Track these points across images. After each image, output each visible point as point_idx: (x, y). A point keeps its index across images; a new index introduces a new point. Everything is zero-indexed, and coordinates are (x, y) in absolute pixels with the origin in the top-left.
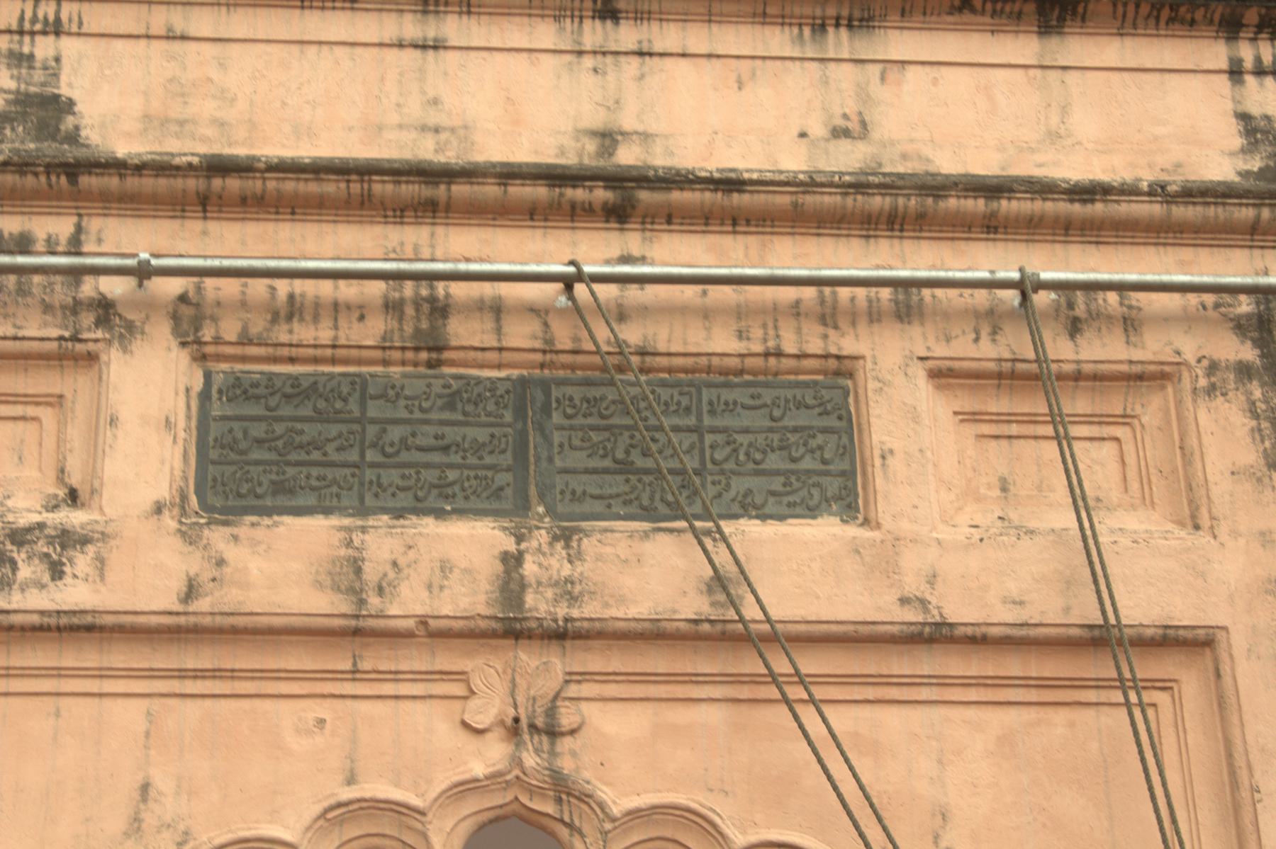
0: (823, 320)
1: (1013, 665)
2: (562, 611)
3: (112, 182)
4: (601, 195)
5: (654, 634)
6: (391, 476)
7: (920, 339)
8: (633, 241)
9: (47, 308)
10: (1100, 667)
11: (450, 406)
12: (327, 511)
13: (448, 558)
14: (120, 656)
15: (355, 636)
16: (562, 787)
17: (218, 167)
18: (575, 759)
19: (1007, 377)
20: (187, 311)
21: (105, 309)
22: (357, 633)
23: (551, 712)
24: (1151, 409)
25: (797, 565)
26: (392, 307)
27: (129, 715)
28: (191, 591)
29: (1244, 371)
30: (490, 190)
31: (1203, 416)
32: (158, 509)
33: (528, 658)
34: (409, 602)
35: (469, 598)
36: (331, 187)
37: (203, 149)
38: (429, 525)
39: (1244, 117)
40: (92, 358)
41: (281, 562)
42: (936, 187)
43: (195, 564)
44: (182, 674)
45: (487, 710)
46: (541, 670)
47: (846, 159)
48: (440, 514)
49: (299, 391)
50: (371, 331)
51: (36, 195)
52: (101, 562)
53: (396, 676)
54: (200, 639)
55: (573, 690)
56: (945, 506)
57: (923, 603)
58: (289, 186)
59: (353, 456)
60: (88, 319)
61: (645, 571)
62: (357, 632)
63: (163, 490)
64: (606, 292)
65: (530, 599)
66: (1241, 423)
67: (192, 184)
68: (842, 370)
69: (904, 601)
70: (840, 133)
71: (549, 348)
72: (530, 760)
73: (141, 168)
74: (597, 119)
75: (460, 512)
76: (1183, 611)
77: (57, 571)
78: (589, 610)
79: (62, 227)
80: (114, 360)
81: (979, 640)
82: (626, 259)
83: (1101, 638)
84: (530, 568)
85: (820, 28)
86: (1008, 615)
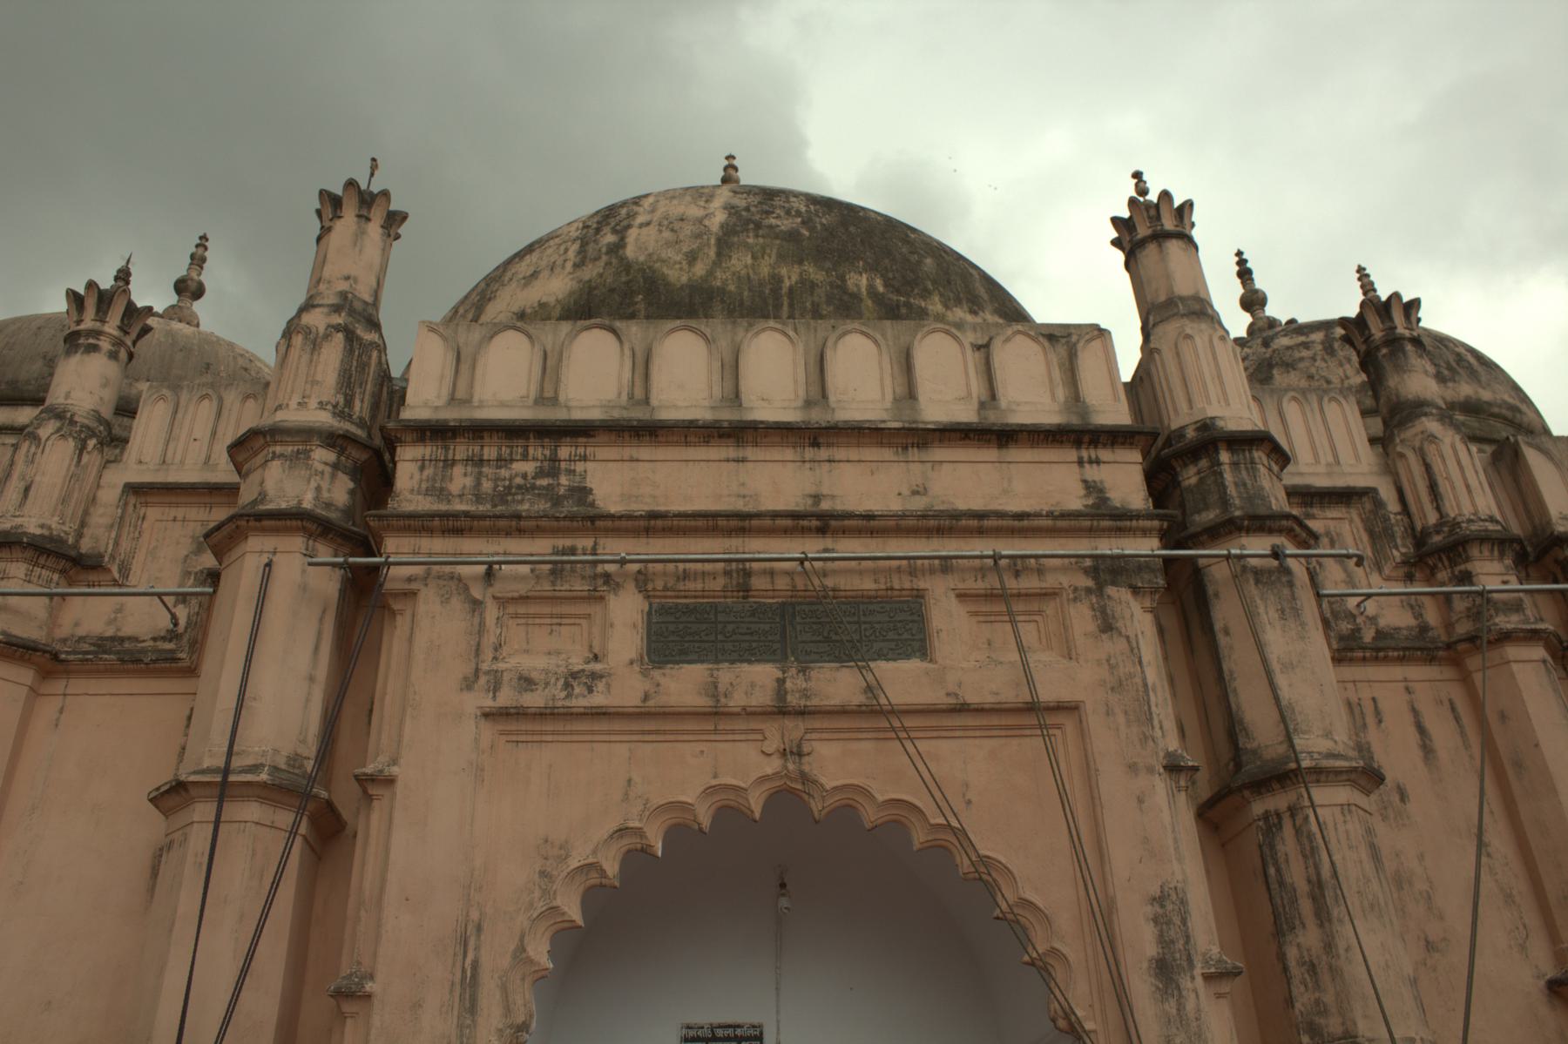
0: (910, 574)
1: (995, 720)
2: (802, 703)
3: (609, 523)
4: (815, 523)
5: (843, 712)
6: (729, 646)
7: (952, 581)
8: (828, 542)
9: (583, 578)
10: (1030, 720)
11: (753, 615)
12: (702, 662)
13: (754, 681)
14: (617, 725)
15: (715, 715)
16: (804, 778)
17: (653, 515)
19: (990, 596)
20: (641, 577)
21: (607, 577)
23: (799, 746)
24: (1050, 608)
25: (902, 680)
26: (727, 573)
27: (622, 750)
28: (646, 698)
29: (1088, 590)
30: (768, 522)
31: (1072, 611)
32: (632, 663)
33: (789, 723)
34: (737, 701)
35: (763, 698)
36: (700, 523)
37: (647, 508)
38: (745, 666)
39: (1085, 481)
40: (602, 598)
41: (684, 684)
42: (956, 515)
43: (648, 686)
44: (643, 732)
45: (772, 745)
46: (795, 728)
47: (918, 504)
48: (750, 662)
49: (689, 610)
50: (720, 583)
51: (578, 530)
52: (608, 686)
53: (733, 732)
55: (808, 736)
56: (966, 652)
57: (956, 695)
58: (683, 523)
59: (712, 638)
60: (600, 581)
61: (837, 684)
62: (716, 713)
63: (633, 655)
64: (817, 564)
65: (789, 698)
66: (1088, 613)
67: (642, 523)
68: (919, 595)
69: (948, 694)
70: (915, 493)
71: (794, 589)
72: (791, 766)
73: (621, 517)
74: (811, 490)
75: (758, 661)
76: (1065, 695)
77: (590, 690)
78: (815, 702)
79: (588, 543)
80: (613, 601)
81: (980, 710)
82: (826, 550)
83: (1032, 708)
84: (788, 684)
85: (905, 448)
86: (991, 699)
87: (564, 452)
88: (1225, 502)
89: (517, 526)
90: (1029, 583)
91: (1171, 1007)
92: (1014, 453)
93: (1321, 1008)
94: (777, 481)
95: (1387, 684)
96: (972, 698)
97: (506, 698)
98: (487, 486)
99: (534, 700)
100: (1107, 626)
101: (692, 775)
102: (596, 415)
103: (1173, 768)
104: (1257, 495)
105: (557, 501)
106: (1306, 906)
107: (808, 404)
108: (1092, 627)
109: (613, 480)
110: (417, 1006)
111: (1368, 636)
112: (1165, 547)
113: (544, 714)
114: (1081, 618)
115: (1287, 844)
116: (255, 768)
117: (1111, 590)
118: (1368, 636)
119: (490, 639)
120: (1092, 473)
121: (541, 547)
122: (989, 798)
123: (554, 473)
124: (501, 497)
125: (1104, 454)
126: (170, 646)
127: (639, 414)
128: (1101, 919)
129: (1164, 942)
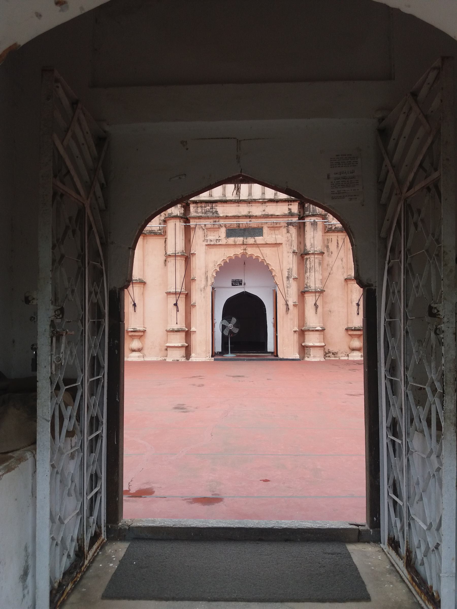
5: (251, 244)
13: (240, 240)
15: (235, 245)
16: (246, 253)
17: (227, 216)
18: (247, 251)
19: (272, 227)
22: (235, 245)
25: (259, 240)
33: (244, 246)
34: (238, 243)
35: (241, 243)
41: (231, 240)
43: (226, 241)
46: (245, 246)
47: (264, 213)
49: (232, 230)
54: (227, 245)
56: (268, 236)
61: (250, 240)
68: (262, 227)
81: (269, 244)
83: (276, 244)
87: (214, 205)
88: (310, 211)
89: (208, 218)
90: (278, 225)
91: (288, 282)
92: (279, 204)
93: (308, 282)
94: (243, 210)
95: (334, 237)
96: (268, 243)
97: (209, 243)
98: (203, 211)
99: (212, 243)
100: (288, 232)
101: (232, 252)
102: (218, 199)
103: (294, 252)
104: (314, 210)
105: (213, 213)
106: (308, 270)
107: (249, 196)
108: (286, 232)
109: (222, 210)
110: (201, 281)
111: (333, 228)
112: (299, 219)
113: (213, 245)
114: (284, 230)
115: (308, 262)
116: (178, 253)
117: (289, 226)
118: (333, 228)
119: (206, 234)
120: (290, 207)
121: (212, 221)
122: (269, 256)
123: (212, 209)
124: (206, 213)
125: (292, 203)
126: (160, 231)
127: (224, 198)
128: (282, 271)
129: (288, 274)
